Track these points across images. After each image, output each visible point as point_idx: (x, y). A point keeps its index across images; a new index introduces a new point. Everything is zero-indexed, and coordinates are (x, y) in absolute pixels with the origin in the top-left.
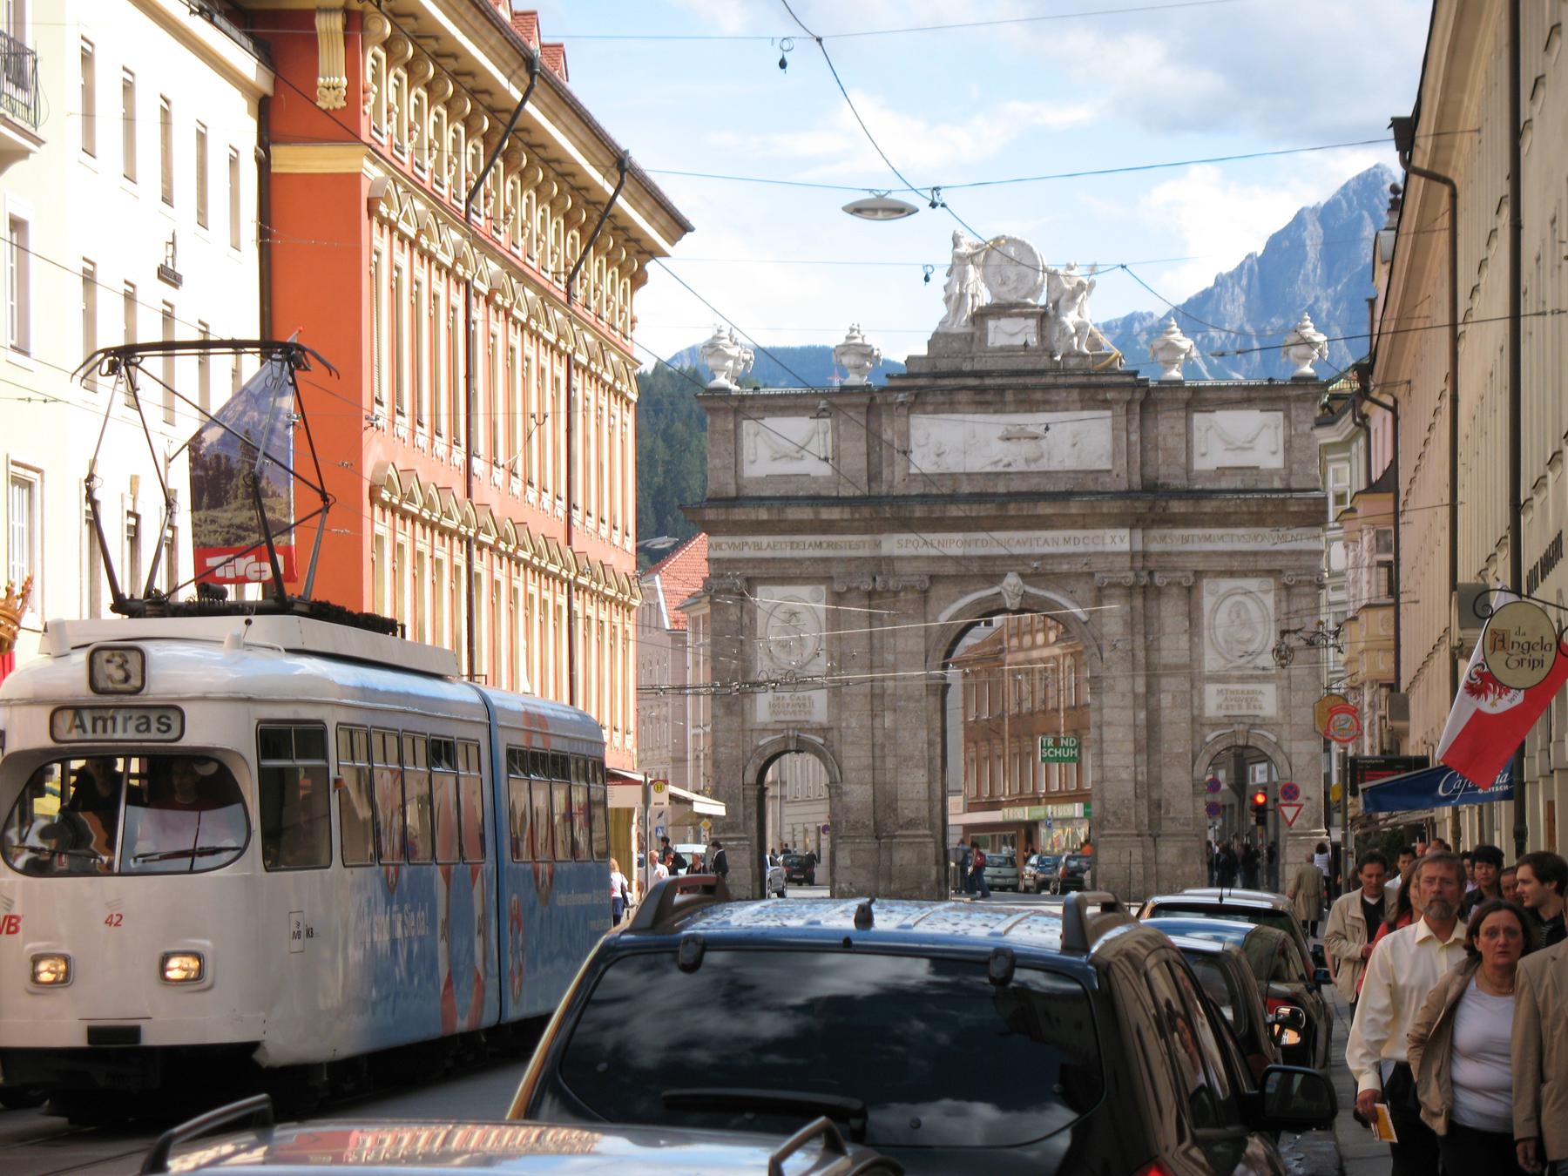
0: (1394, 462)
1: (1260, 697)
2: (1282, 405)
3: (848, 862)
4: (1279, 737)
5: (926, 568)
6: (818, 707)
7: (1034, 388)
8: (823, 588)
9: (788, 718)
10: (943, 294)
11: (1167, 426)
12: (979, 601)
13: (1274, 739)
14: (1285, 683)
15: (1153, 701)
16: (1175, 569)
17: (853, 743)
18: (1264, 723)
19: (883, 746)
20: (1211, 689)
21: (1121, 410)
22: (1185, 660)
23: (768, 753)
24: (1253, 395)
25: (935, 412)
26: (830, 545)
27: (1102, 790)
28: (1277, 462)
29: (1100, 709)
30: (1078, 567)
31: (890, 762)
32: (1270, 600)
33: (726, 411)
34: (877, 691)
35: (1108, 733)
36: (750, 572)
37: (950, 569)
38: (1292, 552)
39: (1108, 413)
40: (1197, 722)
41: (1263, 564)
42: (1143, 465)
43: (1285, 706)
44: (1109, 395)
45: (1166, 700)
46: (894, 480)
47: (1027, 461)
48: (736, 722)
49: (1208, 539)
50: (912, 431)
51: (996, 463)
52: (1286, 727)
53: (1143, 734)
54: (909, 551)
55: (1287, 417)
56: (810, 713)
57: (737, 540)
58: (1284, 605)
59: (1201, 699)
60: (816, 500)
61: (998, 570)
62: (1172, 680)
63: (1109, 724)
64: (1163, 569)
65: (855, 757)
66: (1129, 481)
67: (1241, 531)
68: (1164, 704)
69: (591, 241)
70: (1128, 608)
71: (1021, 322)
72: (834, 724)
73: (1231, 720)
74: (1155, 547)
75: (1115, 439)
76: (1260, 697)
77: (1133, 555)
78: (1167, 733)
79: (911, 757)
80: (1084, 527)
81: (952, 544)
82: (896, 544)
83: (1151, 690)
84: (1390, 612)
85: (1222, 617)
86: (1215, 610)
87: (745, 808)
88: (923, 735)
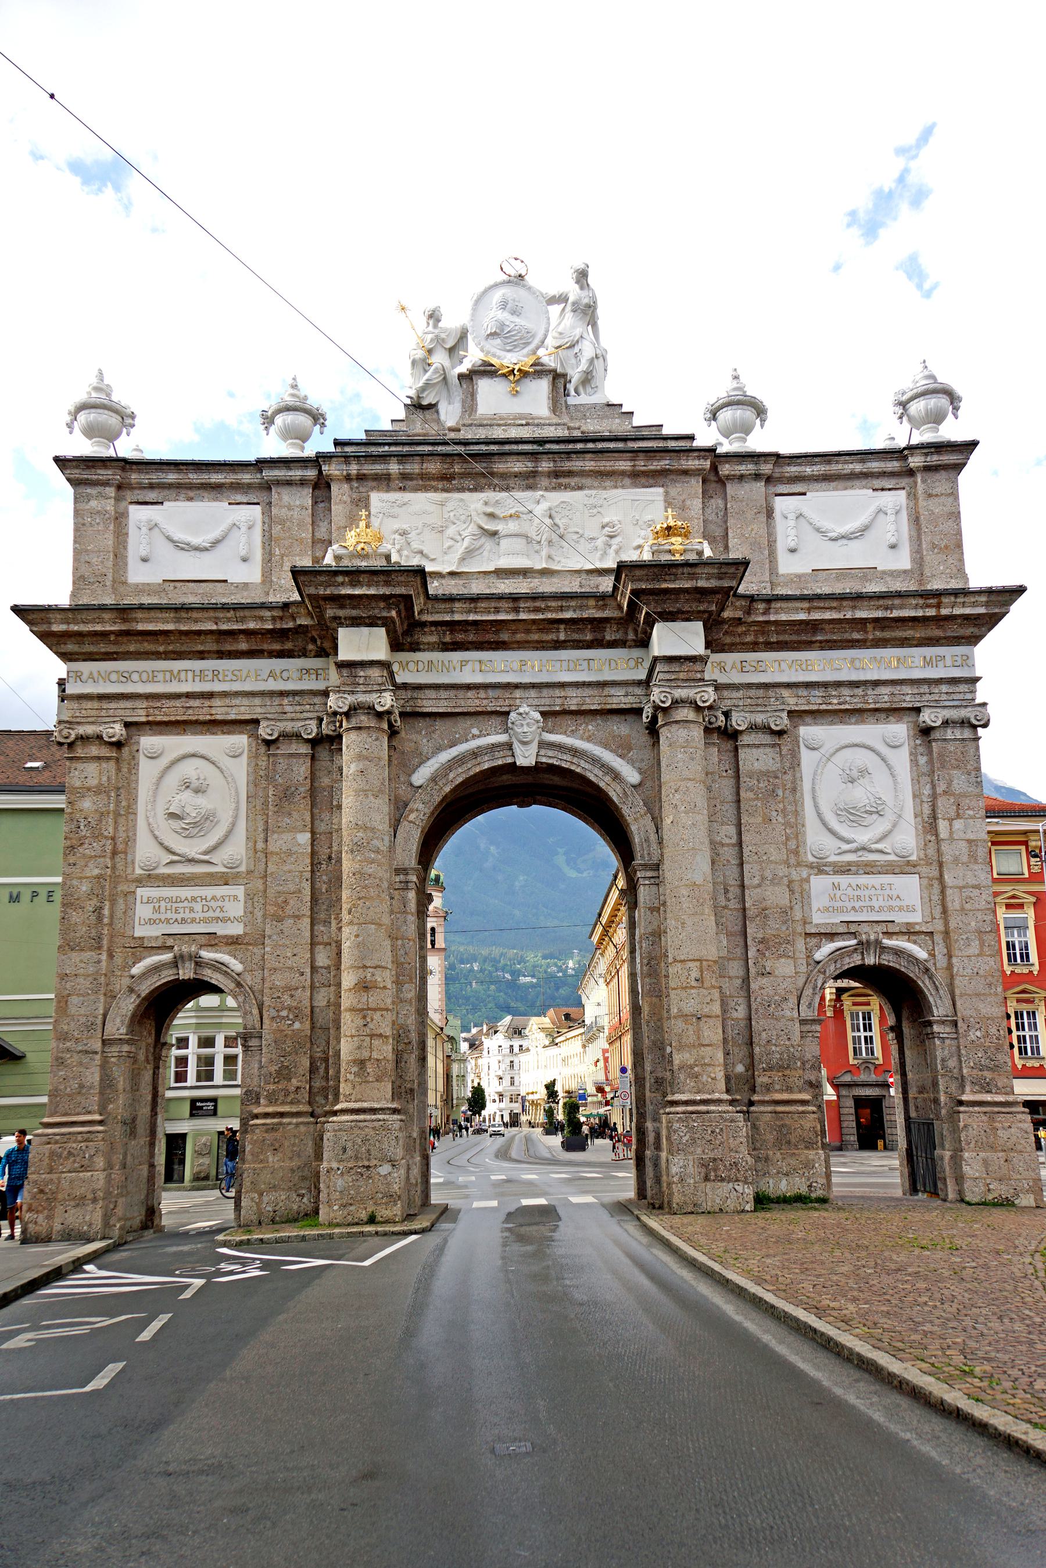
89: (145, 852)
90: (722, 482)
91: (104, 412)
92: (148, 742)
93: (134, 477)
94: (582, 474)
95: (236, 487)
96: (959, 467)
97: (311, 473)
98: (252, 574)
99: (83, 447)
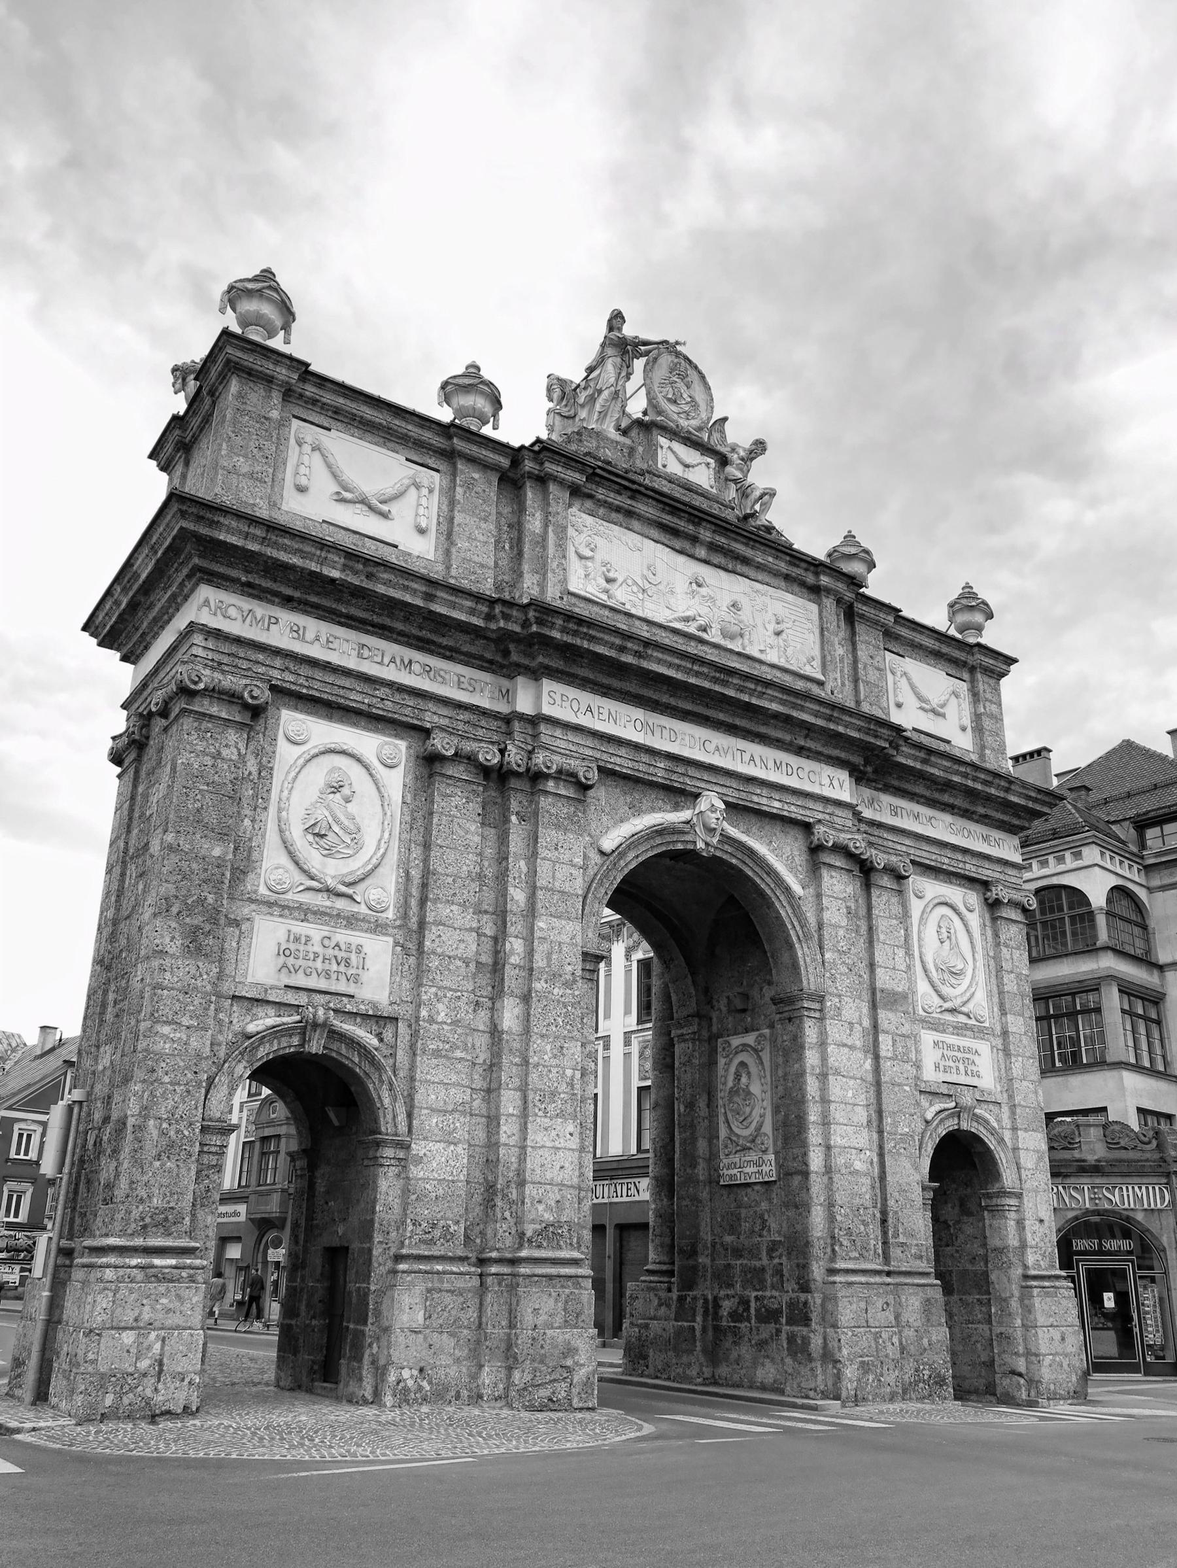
1: (976, 1058)
3: (420, 1316)
8: (402, 745)
9: (312, 982)
12: (660, 831)
14: (999, 1042)
17: (437, 1053)
24: (945, 649)
26: (427, 669)
27: (829, 1187)
30: (795, 812)
31: (509, 1102)
37: (622, 761)
41: (970, 868)
51: (687, 620)
56: (356, 979)
57: (261, 610)
58: (989, 932)
59: (918, 1051)
61: (690, 784)
62: (891, 1015)
63: (837, 1073)
67: (948, 818)
72: (403, 1011)
73: (948, 1091)
76: (976, 1058)
80: (800, 751)
81: (625, 722)
86: (923, 920)
89: (272, 869)
92: (289, 719)
94: (760, 567)
95: (419, 445)
96: (1002, 675)
97: (505, 462)
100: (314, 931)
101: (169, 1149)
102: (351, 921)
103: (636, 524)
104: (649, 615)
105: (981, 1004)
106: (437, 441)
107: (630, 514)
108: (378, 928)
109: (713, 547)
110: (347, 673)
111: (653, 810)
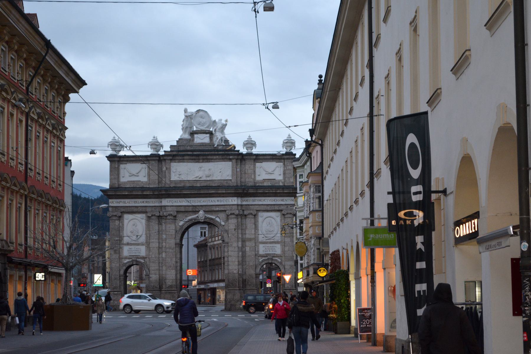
0: (322, 163)
2: (282, 161)
4: (281, 260)
5: (175, 209)
6: (142, 251)
7: (208, 155)
9: (133, 254)
10: (181, 127)
11: (248, 166)
13: (280, 261)
15: (244, 249)
16: (250, 210)
17: (153, 262)
18: (278, 256)
19: (162, 263)
20: (261, 246)
21: (234, 161)
22: (253, 236)
23: (127, 265)
25: (178, 162)
26: (146, 202)
28: (281, 178)
29: (228, 251)
30: (222, 209)
31: (164, 268)
32: (278, 219)
33: (115, 161)
34: (161, 246)
35: (230, 259)
36: (122, 210)
37: (183, 209)
38: (286, 205)
39: (230, 163)
40: (257, 255)
41: (277, 208)
42: (241, 178)
43: (283, 251)
44: (231, 157)
45: (248, 249)
46: (166, 182)
47: (206, 177)
48: (117, 256)
49: (260, 200)
50: (171, 168)
52: (284, 257)
53: (240, 259)
54: (170, 204)
55: (284, 164)
59: (258, 249)
60: (143, 189)
61: (197, 210)
64: (248, 209)
65: (153, 267)
66: (237, 183)
68: (247, 250)
69: (36, 70)
70: (236, 221)
71: (205, 135)
73: (266, 255)
74: (244, 203)
75: (233, 170)
77: (238, 205)
78: (247, 259)
79: (170, 266)
80: (223, 197)
82: (166, 202)
83: (243, 246)
84: (321, 213)
85: (265, 224)
86: (263, 222)
87: (120, 282)
88: (174, 259)
89: (126, 240)
90: (245, 160)
91: (116, 145)
92: (126, 216)
93: (122, 159)
97: (158, 158)
98: (145, 179)
99: (110, 152)
100: (133, 247)
101: (115, 279)
102: (138, 244)
103: (186, 161)
104: (188, 179)
105: (278, 237)
106: (145, 159)
107: (184, 159)
108: (142, 244)
109: (203, 159)
110: (133, 207)
111: (190, 216)
